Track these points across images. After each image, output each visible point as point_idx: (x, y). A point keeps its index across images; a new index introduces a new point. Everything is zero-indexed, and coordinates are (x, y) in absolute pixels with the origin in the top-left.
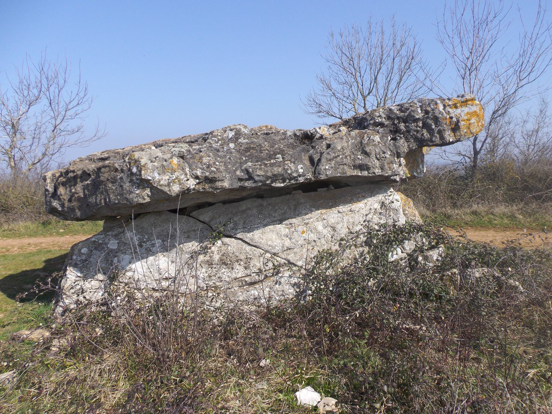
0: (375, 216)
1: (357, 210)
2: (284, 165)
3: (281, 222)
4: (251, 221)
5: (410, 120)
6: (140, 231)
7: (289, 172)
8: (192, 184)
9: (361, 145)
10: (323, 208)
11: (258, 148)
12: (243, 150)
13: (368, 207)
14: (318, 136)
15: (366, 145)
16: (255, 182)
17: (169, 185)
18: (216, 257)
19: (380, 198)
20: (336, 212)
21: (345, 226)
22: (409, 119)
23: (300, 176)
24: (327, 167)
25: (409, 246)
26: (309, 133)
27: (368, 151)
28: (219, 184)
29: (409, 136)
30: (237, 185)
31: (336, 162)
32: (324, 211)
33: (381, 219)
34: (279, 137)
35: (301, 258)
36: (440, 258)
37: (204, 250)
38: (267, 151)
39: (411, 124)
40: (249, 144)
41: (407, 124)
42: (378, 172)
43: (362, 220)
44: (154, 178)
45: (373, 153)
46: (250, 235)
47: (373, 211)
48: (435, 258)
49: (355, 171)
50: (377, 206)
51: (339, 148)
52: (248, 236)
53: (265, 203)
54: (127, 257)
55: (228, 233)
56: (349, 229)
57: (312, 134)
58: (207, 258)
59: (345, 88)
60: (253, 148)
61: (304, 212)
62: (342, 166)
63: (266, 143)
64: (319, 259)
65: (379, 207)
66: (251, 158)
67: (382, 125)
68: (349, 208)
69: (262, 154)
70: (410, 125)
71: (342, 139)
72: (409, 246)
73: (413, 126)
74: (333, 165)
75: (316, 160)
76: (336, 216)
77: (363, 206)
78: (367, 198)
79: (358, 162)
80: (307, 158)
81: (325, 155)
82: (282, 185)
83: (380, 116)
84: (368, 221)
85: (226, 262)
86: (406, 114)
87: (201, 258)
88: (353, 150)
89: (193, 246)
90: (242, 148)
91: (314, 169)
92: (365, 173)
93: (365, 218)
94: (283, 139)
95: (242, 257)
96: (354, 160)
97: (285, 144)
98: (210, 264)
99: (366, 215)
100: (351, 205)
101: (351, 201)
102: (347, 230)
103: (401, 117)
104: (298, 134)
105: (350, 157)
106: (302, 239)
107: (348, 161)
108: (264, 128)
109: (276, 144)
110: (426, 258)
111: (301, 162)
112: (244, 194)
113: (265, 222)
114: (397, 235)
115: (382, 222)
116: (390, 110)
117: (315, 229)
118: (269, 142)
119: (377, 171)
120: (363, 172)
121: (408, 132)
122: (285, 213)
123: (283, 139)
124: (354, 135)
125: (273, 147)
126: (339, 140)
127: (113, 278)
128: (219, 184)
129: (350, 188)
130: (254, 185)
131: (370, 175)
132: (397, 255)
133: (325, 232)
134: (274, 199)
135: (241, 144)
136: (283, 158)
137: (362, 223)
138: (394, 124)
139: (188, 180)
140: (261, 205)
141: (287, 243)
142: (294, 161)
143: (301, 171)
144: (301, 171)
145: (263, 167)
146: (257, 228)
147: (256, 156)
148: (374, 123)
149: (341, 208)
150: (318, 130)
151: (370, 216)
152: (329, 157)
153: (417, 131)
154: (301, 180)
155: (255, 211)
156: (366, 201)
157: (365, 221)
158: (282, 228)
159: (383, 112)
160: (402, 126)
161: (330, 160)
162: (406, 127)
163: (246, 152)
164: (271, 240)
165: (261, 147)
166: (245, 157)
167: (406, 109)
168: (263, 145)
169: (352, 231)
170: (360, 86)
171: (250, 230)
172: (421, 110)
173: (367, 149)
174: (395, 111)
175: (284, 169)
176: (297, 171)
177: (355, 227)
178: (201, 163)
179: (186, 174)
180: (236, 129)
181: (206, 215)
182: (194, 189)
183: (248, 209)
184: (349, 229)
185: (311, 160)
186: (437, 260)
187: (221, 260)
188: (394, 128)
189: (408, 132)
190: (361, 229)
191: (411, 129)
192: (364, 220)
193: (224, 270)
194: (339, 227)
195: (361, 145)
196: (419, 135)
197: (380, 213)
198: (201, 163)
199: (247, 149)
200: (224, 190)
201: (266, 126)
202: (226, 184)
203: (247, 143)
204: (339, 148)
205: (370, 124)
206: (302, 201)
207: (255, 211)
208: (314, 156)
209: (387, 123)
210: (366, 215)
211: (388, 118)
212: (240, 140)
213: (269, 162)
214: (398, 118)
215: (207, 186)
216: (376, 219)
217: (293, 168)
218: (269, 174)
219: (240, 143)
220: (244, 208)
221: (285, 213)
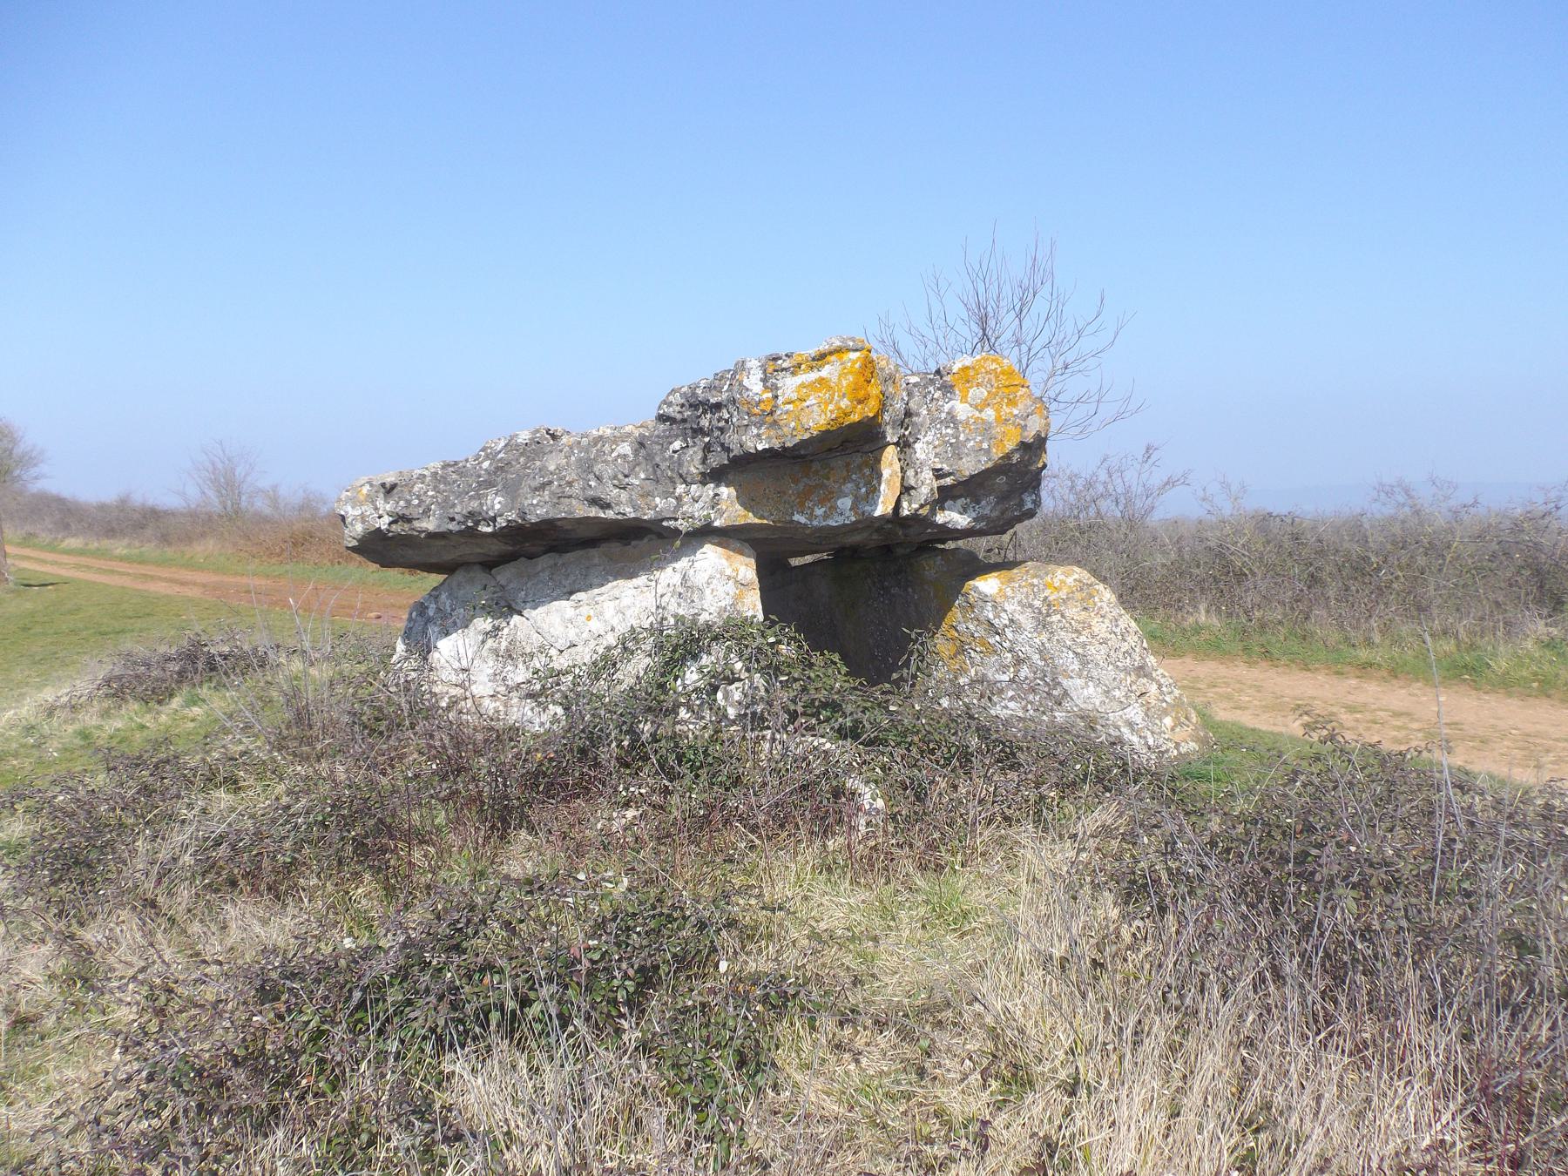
8: (383, 524)
28: (416, 524)
31: (552, 493)
32: (621, 582)
46: (534, 613)
61: (596, 581)
82: (489, 530)
87: (490, 642)
92: (610, 514)
98: (496, 652)
115: (681, 612)
128: (416, 524)
133: (615, 622)
141: (572, 634)
143: (497, 507)
144: (497, 507)
146: (542, 603)
149: (641, 580)
152: (535, 484)
154: (501, 522)
155: (545, 575)
158: (563, 607)
161: (536, 489)
179: (376, 509)
183: (543, 570)
187: (508, 650)
194: (628, 613)
202: (430, 525)
204: (552, 468)
215: (406, 527)
216: (673, 607)
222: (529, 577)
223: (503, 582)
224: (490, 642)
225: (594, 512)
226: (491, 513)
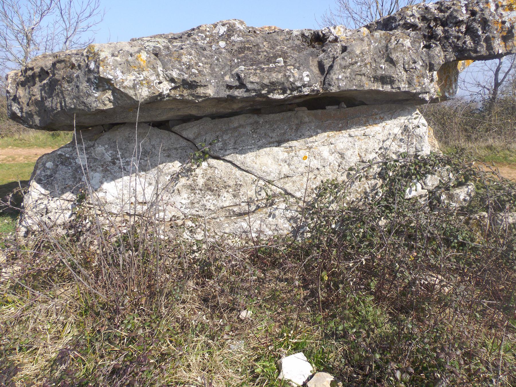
0: (393, 143)
1: (372, 134)
2: (285, 71)
3: (279, 143)
4: (243, 141)
5: (451, 23)
6: (112, 146)
7: (291, 80)
8: (165, 88)
9: (387, 51)
10: (331, 130)
11: (255, 49)
12: (236, 51)
13: (386, 132)
14: (331, 38)
15: (392, 51)
16: (248, 91)
17: (134, 87)
18: (201, 181)
19: (402, 121)
20: (347, 135)
21: (357, 153)
22: (449, 21)
23: (304, 86)
24: (340, 77)
25: (432, 181)
26: (320, 33)
27: (394, 59)
28: (201, 91)
29: (448, 44)
30: (225, 93)
31: (353, 71)
32: (331, 133)
33: (400, 146)
34: (283, 37)
35: (301, 188)
36: (468, 198)
37: (187, 172)
38: (265, 53)
39: (451, 27)
40: (244, 42)
41: (446, 28)
42: (404, 87)
43: (377, 147)
44: (116, 78)
45: (401, 62)
47: (392, 137)
48: (462, 197)
49: (376, 84)
50: (397, 131)
51: (358, 52)
52: (238, 159)
53: (261, 121)
54: (98, 176)
55: (216, 154)
56: (360, 156)
57: (324, 35)
58: (190, 182)
59: (364, 9)
60: (248, 48)
61: (308, 133)
62: (359, 77)
63: (265, 43)
64: (322, 191)
65: (400, 131)
66: (244, 61)
67: (414, 27)
68: (363, 132)
69: (259, 57)
70: (450, 30)
71: (362, 40)
72: (432, 181)
73: (453, 31)
74: (348, 75)
75: (327, 66)
76: (347, 140)
77: (381, 130)
78: (386, 120)
79: (380, 73)
80: (316, 63)
81: (339, 61)
82: (282, 97)
83: (413, 15)
84: (386, 149)
85: (212, 187)
86: (446, 15)
87: (183, 181)
88: (375, 56)
89: (176, 166)
90: (235, 48)
91: (323, 78)
92: (388, 88)
93: (381, 144)
94: (288, 40)
95: (231, 183)
96: (375, 70)
97: (289, 46)
98: (192, 189)
99: (384, 141)
100: (365, 128)
101: (365, 124)
102: (359, 158)
103: (439, 18)
104: (307, 35)
105: (371, 66)
106: (303, 165)
107: (367, 70)
108: (267, 29)
109: (277, 45)
110: (451, 197)
111: (308, 68)
112: (236, 106)
113: (260, 143)
114: (419, 168)
115: (402, 150)
116: (427, 8)
117: (319, 154)
118: (269, 42)
119: (403, 85)
120: (385, 86)
121: (447, 38)
122: (284, 134)
123: (288, 40)
124: (379, 36)
125: (274, 48)
126: (358, 42)
127: (82, 198)
128: (201, 91)
129: (366, 107)
130: (245, 95)
131: (394, 91)
132: (416, 191)
134: (272, 116)
135: (233, 43)
136: (285, 62)
137: (377, 150)
138: (429, 27)
139: (160, 83)
140: (257, 123)
141: (285, 170)
142: (299, 67)
143: (306, 79)
144: (306, 79)
145: (258, 71)
146: (251, 150)
147: (251, 59)
148: (404, 24)
149: (353, 131)
150: (333, 30)
151: (388, 143)
152: (344, 63)
153: (458, 38)
154: (306, 91)
155: (248, 129)
156: (384, 124)
157: (381, 148)
158: (279, 152)
159: (417, 11)
160: (439, 30)
161: (345, 67)
162: (445, 31)
163: (240, 53)
164: (266, 165)
165: (259, 48)
166: (238, 59)
167: (447, 8)
168: (261, 45)
169: (365, 159)
170: (380, 7)
171: (242, 152)
172: (467, 10)
173: (394, 56)
174: (433, 10)
175: (285, 75)
176: (301, 79)
177: (368, 155)
178: (180, 62)
179: (158, 75)
180: (229, 24)
181: (190, 131)
182: (168, 95)
183: (241, 126)
184: (360, 156)
185: (321, 66)
186: (465, 200)
188: (428, 32)
189: (447, 38)
190: (376, 158)
191: (451, 35)
192: (380, 146)
193: (209, 197)
194: (348, 154)
195: (387, 51)
196: (460, 43)
197: (401, 140)
198: (180, 62)
199: (242, 50)
200: (207, 99)
201: (270, 27)
202: (210, 92)
203: (241, 42)
205: (399, 25)
206: (307, 120)
207: (248, 129)
208: (325, 62)
209: (420, 25)
210: (384, 141)
211: (424, 18)
212: (232, 38)
213: (267, 66)
214: (435, 19)
215: (186, 93)
216: (394, 147)
217: (297, 75)
218: (266, 81)
219: (233, 41)
220: (236, 125)
221: (284, 134)
222: (225, 132)
223: (191, 136)
224: (183, 181)
225: (377, 87)
226: (298, 84)
